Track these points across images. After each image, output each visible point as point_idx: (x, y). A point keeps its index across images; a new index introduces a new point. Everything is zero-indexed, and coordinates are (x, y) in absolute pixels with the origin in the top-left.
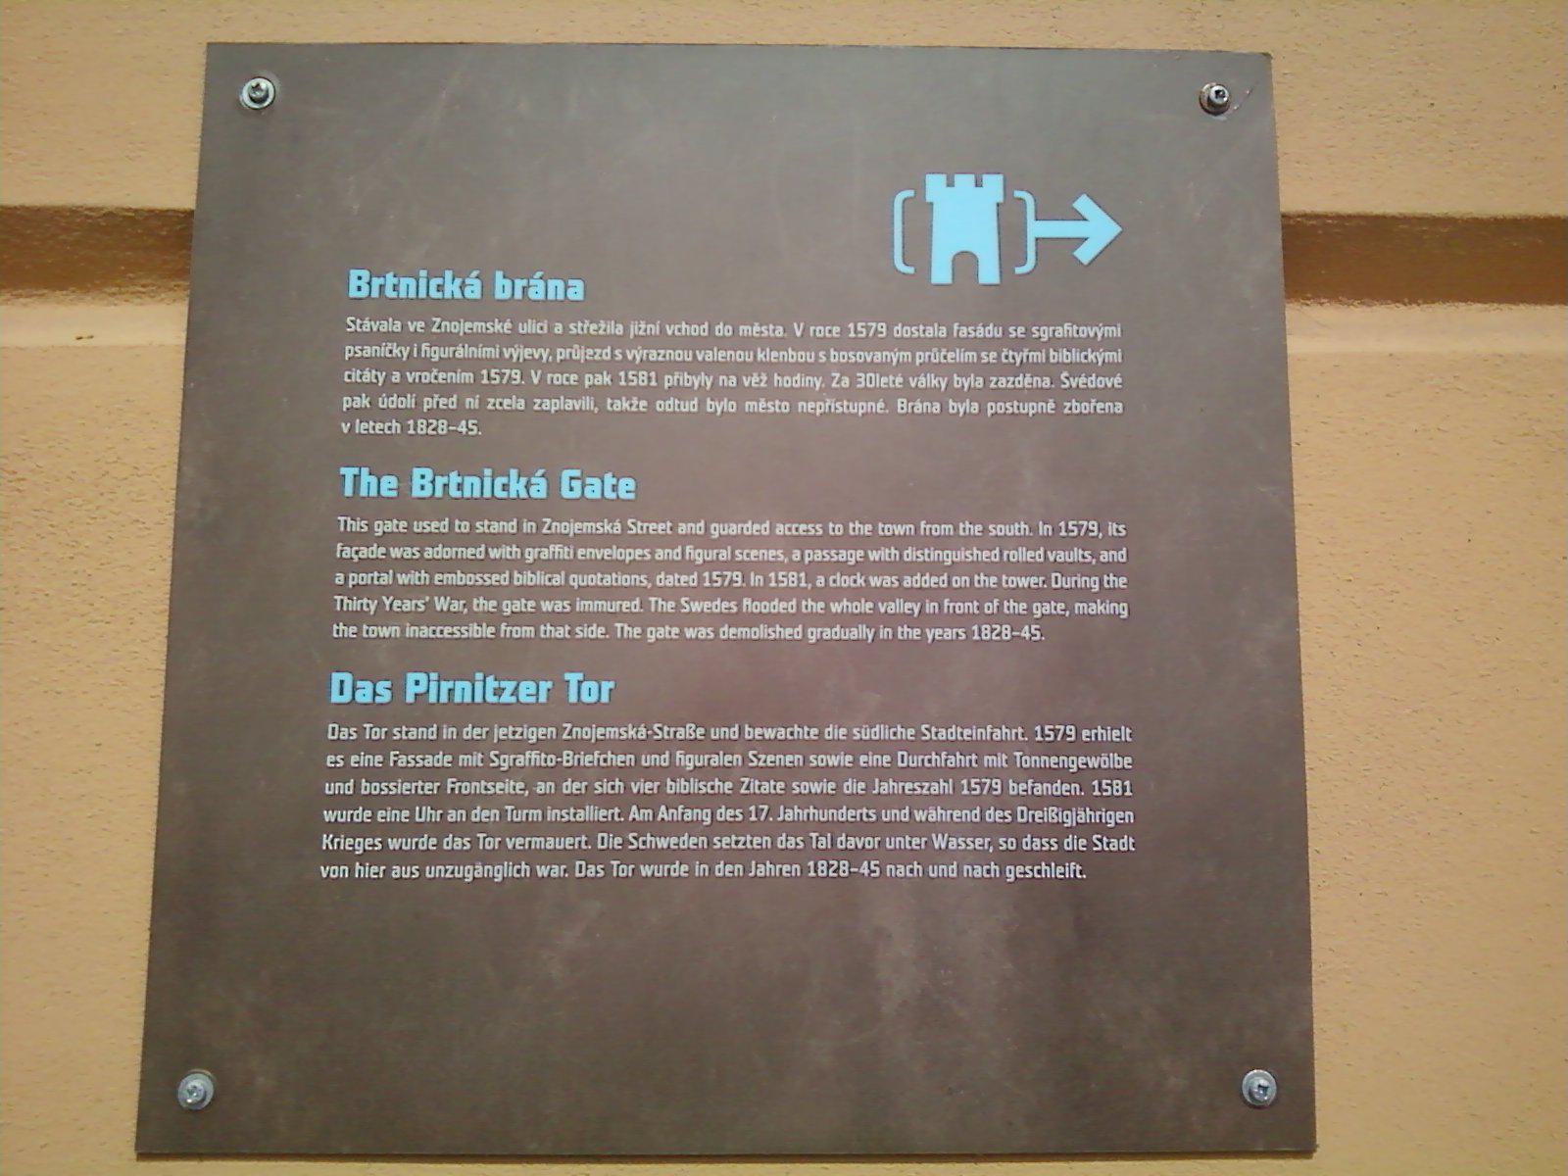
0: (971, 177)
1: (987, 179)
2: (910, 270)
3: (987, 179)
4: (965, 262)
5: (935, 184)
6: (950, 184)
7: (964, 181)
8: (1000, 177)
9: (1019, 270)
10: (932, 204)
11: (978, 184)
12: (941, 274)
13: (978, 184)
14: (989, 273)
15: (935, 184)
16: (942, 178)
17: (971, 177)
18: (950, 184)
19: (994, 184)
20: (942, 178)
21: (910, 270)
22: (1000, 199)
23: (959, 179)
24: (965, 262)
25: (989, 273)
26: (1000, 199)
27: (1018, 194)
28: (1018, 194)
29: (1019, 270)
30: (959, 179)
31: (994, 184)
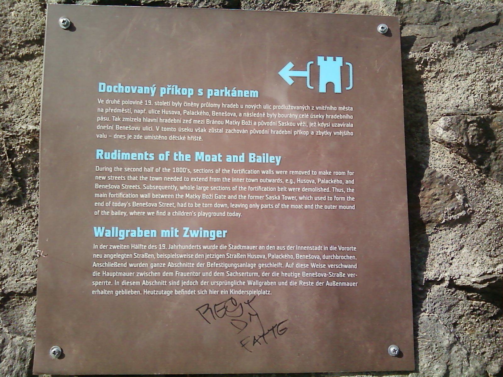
0: (332, 58)
1: (337, 58)
2: (312, 88)
3: (337, 58)
4: (330, 85)
5: (320, 59)
6: (325, 60)
7: (330, 59)
8: (341, 58)
9: (347, 89)
10: (319, 66)
11: (335, 60)
12: (322, 89)
13: (335, 60)
14: (338, 89)
15: (320, 59)
16: (323, 58)
17: (332, 58)
18: (325, 60)
19: (340, 60)
20: (323, 58)
21: (312, 88)
22: (342, 65)
23: (328, 58)
24: (330, 85)
25: (338, 89)
26: (342, 65)
27: (347, 63)
28: (347, 63)
29: (347, 89)
30: (328, 58)
31: (340, 60)
